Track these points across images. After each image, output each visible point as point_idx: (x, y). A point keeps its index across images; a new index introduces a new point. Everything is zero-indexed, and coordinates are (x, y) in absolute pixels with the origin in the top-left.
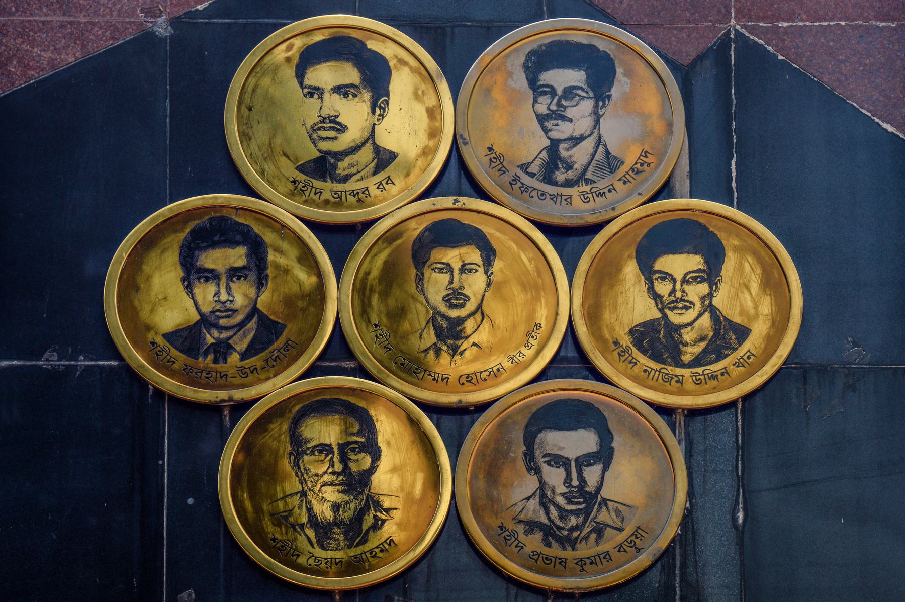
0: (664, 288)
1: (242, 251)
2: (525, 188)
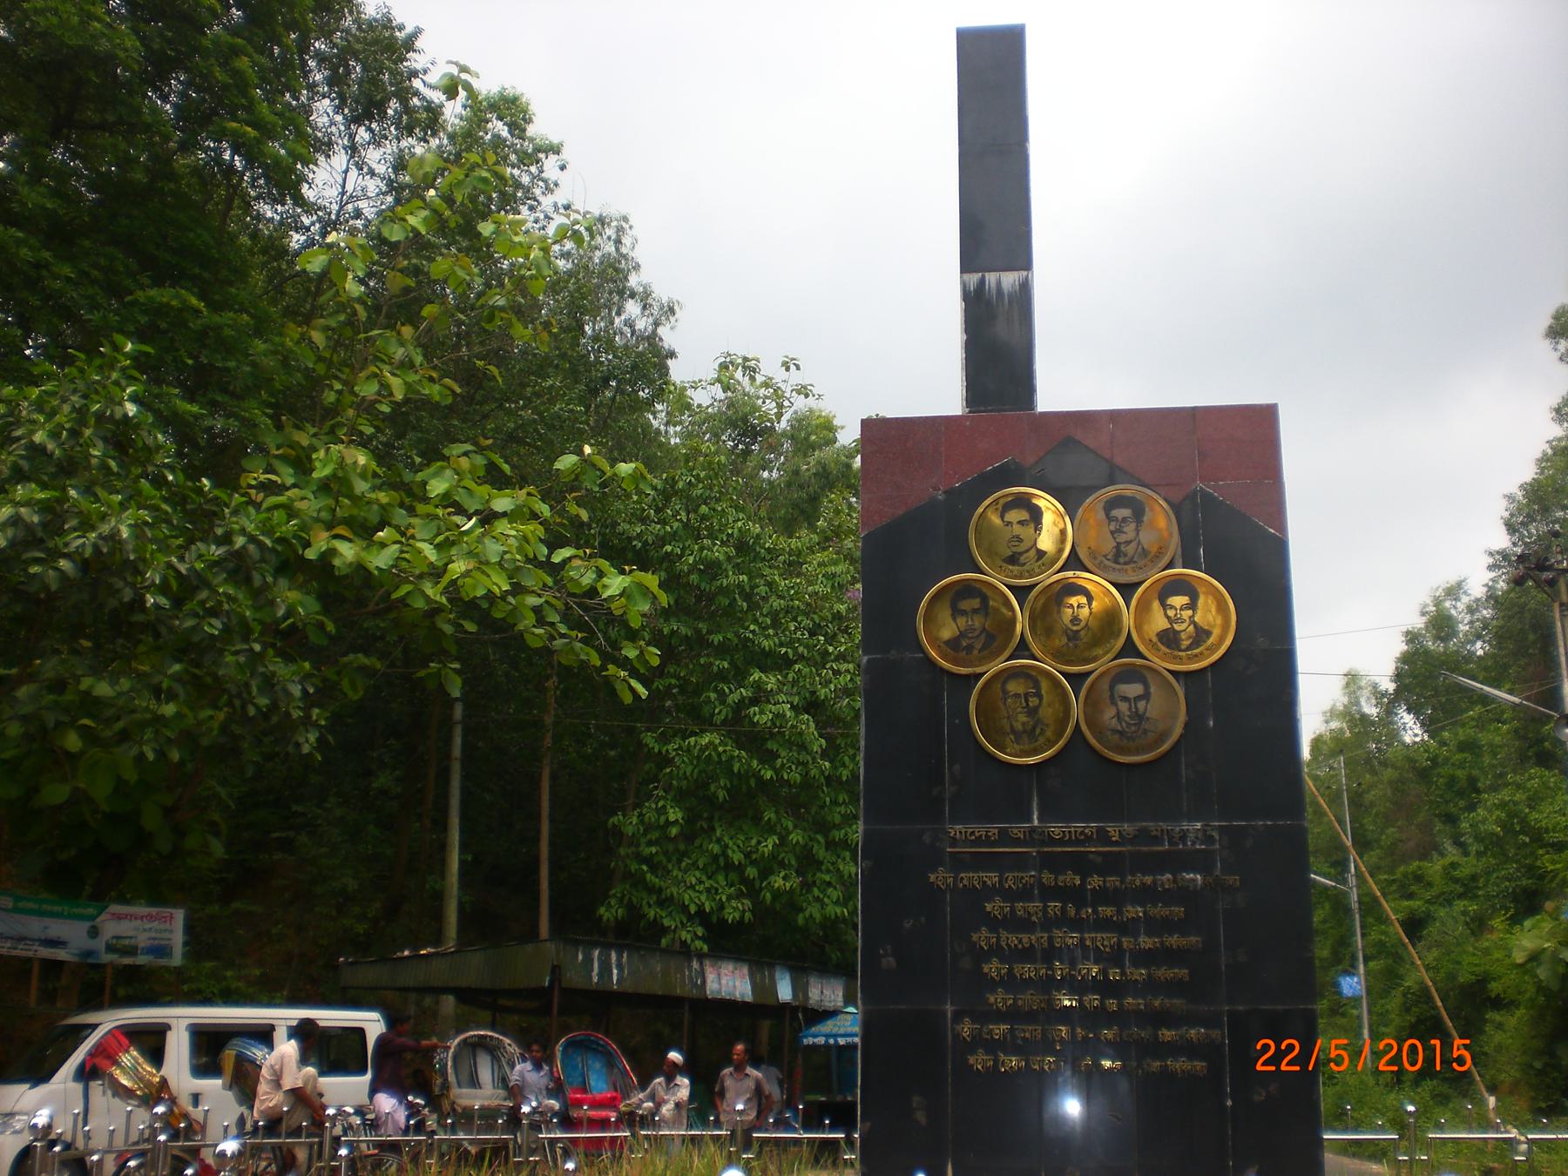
0: (1171, 613)
1: (978, 600)
2: (1105, 567)
